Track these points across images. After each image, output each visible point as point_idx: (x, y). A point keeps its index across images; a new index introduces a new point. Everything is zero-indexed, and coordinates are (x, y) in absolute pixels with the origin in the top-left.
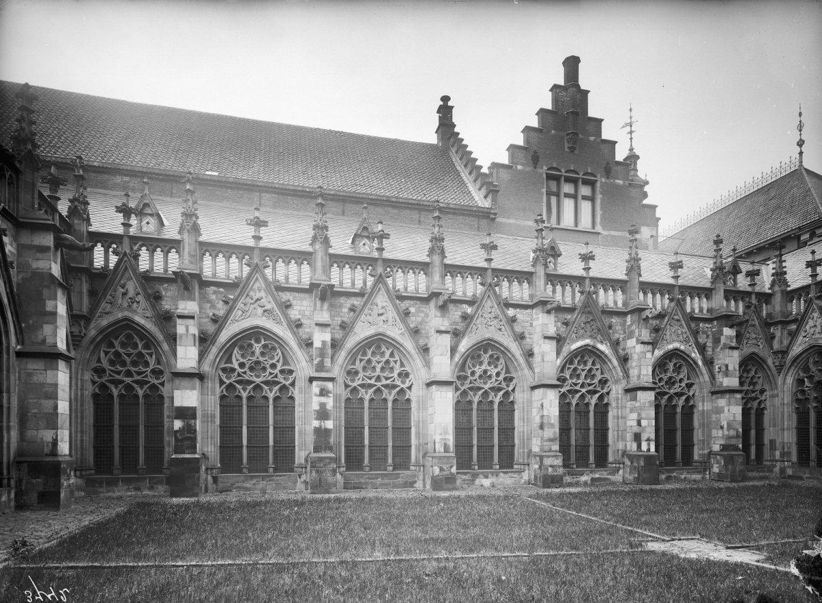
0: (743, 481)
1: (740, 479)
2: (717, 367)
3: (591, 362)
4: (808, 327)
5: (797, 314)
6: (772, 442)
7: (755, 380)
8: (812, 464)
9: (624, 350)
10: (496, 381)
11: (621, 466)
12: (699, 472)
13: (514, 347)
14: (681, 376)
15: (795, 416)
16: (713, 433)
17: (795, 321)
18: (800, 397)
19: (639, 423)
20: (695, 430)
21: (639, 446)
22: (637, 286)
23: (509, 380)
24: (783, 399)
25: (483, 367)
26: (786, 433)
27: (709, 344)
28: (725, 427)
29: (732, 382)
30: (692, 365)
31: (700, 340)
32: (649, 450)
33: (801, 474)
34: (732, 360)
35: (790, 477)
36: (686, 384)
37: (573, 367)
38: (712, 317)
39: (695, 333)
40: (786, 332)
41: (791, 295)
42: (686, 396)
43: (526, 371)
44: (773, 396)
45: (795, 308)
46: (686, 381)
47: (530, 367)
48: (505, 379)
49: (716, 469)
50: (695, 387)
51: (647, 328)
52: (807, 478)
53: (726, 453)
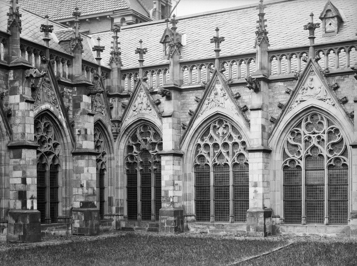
0: (97, 234)
1: (96, 232)
2: (77, 130)
4: (136, 103)
5: (129, 91)
6: (110, 199)
7: (99, 144)
8: (139, 217)
9: (7, 105)
11: (6, 224)
12: (64, 228)
14: (50, 136)
15: (126, 176)
16: (74, 191)
17: (127, 96)
18: (130, 161)
19: (24, 181)
20: (60, 189)
21: (24, 204)
22: (19, 41)
24: (117, 162)
26: (119, 190)
27: (71, 108)
28: (85, 185)
29: (89, 145)
30: (58, 127)
31: (65, 103)
32: (32, 208)
33: (132, 226)
34: (89, 124)
35: (123, 229)
36: (53, 144)
38: (73, 83)
39: (61, 96)
40: (120, 105)
41: (124, 73)
42: (53, 155)
44: (110, 159)
45: (128, 85)
46: (54, 142)
49: (77, 224)
50: (59, 147)
51: (29, 87)
52: (137, 229)
53: (86, 209)
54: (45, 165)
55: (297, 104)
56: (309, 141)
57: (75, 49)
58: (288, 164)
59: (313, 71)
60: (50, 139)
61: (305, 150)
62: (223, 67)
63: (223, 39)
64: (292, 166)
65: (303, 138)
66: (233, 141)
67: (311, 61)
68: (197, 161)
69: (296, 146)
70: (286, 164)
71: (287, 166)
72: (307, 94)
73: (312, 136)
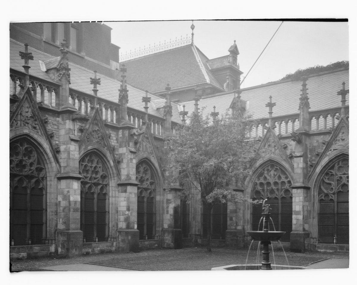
3: (96, 162)
10: (30, 170)
13: (46, 145)
14: (147, 177)
23: (40, 170)
25: (20, 157)
36: (150, 182)
37: (84, 164)
43: (54, 164)
47: (57, 161)
48: (37, 169)
54: (143, 197)
55: (331, 152)
56: (340, 180)
57: (166, 114)
58: (323, 198)
59: (344, 126)
60: (147, 179)
61: (337, 186)
62: (275, 125)
63: (274, 104)
64: (326, 199)
65: (336, 178)
66: (282, 180)
67: (342, 119)
68: (254, 194)
69: (330, 184)
70: (322, 198)
71: (322, 200)
72: (339, 144)
73: (342, 176)
